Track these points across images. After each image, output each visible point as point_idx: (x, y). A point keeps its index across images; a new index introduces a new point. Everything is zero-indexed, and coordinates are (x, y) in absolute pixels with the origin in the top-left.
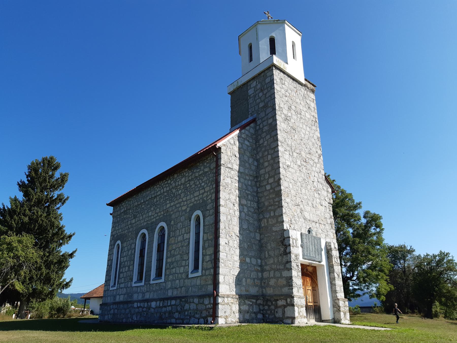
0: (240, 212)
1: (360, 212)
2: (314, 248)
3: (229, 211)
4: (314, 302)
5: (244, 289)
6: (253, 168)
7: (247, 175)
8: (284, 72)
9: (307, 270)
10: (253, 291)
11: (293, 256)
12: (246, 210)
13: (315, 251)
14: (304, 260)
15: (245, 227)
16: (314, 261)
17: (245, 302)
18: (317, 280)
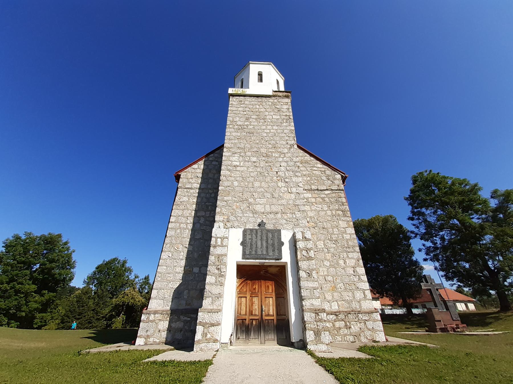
0: (194, 224)
1: (485, 194)
2: (264, 244)
3: (180, 225)
4: (277, 314)
5: (185, 302)
7: (210, 189)
8: (245, 96)
9: (267, 272)
11: (212, 259)
12: (202, 220)
13: (267, 247)
14: (245, 260)
16: (265, 259)
17: (179, 317)
18: (286, 283)
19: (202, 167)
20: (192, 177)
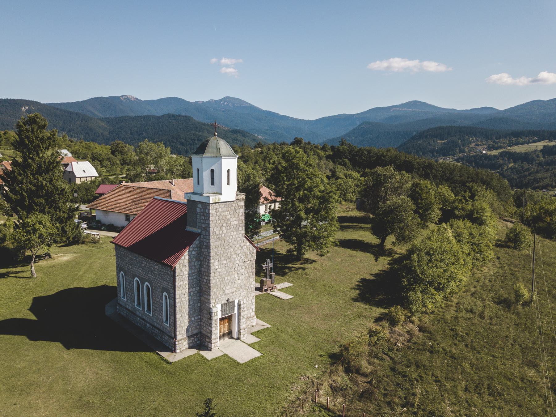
6: (197, 267)
10: (195, 332)
12: (192, 294)
15: (191, 303)
19: (187, 257)
20: (183, 265)
